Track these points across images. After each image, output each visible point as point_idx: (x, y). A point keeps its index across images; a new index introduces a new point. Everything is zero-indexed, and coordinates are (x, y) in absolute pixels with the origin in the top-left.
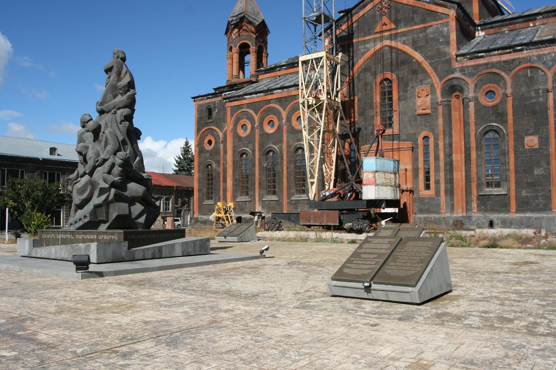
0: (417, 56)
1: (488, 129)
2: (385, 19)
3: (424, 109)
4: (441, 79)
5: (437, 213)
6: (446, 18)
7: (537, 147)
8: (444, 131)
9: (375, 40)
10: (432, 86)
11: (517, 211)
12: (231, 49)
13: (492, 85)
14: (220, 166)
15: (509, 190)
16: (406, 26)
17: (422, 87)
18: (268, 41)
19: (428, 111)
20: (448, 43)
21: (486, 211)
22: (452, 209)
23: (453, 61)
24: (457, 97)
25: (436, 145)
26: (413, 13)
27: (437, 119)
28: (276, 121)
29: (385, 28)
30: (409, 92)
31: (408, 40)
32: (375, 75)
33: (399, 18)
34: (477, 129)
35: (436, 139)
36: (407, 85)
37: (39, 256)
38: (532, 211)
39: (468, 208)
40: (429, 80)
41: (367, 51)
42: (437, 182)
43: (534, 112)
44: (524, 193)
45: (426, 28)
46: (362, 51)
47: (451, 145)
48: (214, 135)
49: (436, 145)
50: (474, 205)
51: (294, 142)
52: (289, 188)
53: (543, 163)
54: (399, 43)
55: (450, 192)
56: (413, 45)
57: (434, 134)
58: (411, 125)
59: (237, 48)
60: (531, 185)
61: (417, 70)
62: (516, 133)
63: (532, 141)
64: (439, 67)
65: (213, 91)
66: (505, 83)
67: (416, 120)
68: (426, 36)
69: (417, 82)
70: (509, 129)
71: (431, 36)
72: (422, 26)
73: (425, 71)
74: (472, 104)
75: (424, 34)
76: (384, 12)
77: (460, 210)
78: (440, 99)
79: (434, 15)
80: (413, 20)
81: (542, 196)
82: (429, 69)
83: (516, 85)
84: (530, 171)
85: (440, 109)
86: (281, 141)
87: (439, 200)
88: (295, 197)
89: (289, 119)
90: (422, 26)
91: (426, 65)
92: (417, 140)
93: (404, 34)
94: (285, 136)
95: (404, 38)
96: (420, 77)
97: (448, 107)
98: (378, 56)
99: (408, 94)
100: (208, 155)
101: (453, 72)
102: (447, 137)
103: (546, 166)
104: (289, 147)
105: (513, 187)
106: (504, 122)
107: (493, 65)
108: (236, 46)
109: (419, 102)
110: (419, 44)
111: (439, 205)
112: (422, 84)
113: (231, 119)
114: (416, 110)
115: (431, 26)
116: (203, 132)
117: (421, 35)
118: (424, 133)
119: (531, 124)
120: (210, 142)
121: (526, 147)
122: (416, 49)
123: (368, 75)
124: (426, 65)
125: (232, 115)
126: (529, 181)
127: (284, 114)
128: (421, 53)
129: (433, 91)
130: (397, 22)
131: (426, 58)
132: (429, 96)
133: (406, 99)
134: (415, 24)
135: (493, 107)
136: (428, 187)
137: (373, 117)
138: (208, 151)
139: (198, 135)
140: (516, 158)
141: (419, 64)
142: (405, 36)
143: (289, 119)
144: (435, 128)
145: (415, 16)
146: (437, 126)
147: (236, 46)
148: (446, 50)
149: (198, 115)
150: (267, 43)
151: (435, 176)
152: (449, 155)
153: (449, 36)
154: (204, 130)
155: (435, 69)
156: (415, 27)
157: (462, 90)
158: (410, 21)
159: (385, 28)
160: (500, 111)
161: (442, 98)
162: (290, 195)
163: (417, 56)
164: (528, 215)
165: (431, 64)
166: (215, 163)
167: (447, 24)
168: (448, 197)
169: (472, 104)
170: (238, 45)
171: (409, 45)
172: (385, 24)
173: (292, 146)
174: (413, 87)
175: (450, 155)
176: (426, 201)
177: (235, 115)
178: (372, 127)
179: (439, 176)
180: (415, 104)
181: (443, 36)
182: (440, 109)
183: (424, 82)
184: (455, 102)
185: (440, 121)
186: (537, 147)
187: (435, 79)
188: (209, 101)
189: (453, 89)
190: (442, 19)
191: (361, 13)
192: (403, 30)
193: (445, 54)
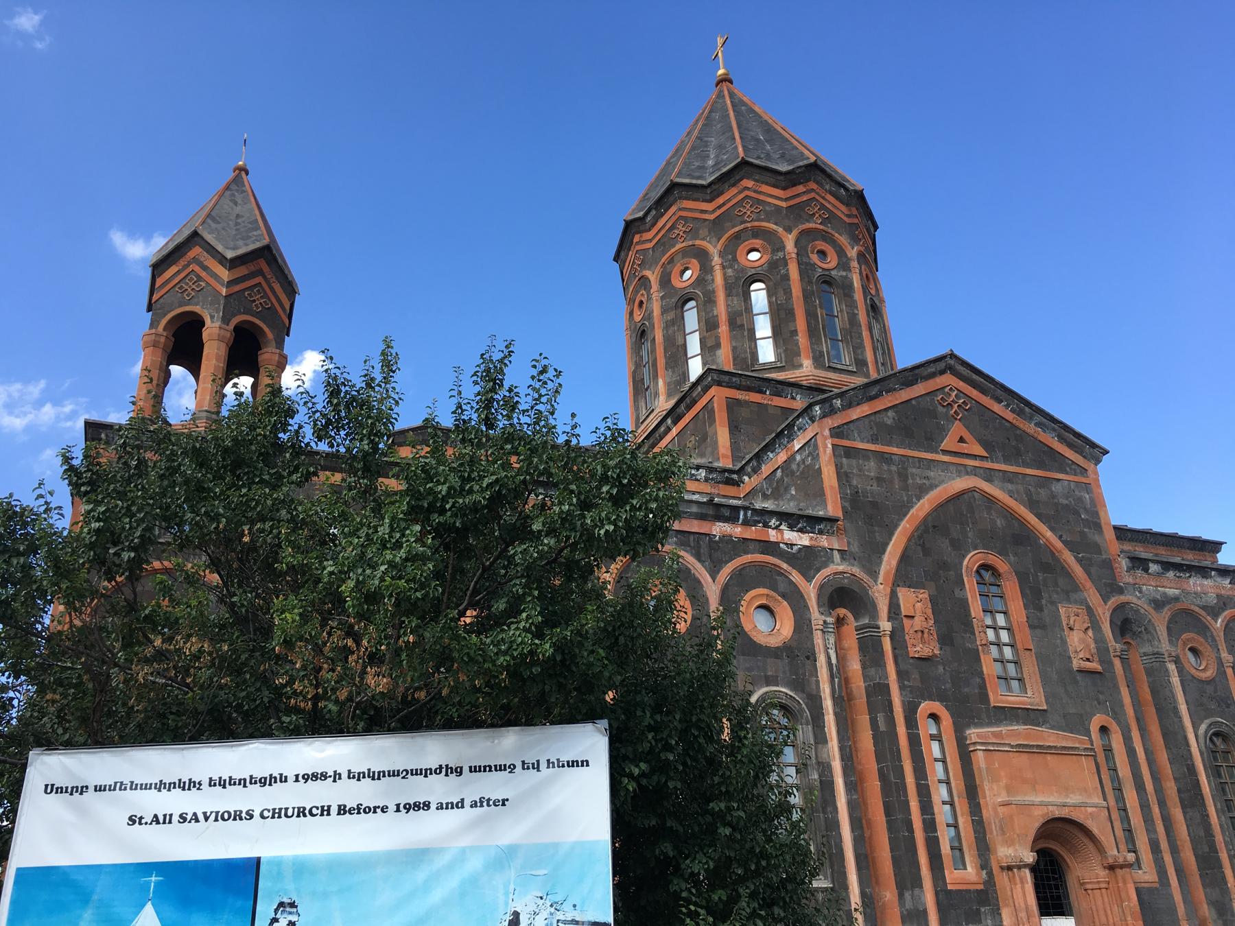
2: (957, 429)
3: (1088, 660)
4: (1105, 599)
6: (1082, 474)
10: (1090, 611)
16: (1007, 460)
27: (1116, 687)
29: (964, 448)
30: (1046, 611)
32: (960, 548)
35: (1127, 739)
49: (1131, 752)
57: (1119, 723)
59: (231, 327)
61: (1051, 565)
69: (1057, 593)
73: (1067, 574)
82: (1078, 570)
93: (1008, 478)
95: (1010, 486)
101: (1121, 591)
131: (1069, 545)
132: (1090, 633)
142: (1010, 481)
148: (1097, 538)
165: (1079, 561)
171: (1022, 502)
172: (962, 440)
174: (1053, 603)
179: (1156, 832)
180: (1064, 642)
187: (1092, 596)
192: (1004, 467)
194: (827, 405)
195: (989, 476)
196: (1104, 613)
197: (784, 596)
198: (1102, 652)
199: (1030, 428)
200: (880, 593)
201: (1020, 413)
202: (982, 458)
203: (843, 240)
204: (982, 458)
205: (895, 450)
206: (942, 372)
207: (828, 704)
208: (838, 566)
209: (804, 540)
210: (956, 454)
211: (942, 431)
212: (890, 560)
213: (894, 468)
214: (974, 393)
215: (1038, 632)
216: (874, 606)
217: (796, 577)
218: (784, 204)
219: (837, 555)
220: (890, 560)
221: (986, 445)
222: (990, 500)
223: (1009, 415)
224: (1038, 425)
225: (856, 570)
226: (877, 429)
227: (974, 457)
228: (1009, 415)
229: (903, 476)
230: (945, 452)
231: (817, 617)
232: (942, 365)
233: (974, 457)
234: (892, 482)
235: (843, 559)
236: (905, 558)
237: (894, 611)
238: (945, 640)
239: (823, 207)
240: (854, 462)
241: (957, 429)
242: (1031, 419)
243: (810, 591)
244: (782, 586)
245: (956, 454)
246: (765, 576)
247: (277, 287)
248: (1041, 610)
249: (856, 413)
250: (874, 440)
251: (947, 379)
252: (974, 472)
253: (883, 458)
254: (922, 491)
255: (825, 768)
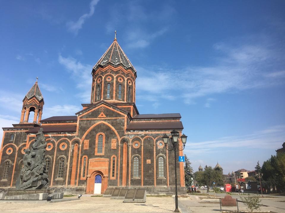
0: (113, 128)
1: (135, 156)
2: (102, 113)
4: (121, 137)
5: (116, 185)
7: (150, 163)
8: (120, 156)
9: (98, 120)
10: (117, 139)
11: (144, 185)
12: (25, 108)
13: (137, 141)
14: (14, 163)
15: (141, 178)
16: (110, 117)
17: (114, 139)
18: (43, 107)
19: (116, 148)
20: (124, 126)
21: (133, 185)
22: (121, 184)
23: (125, 132)
24: (126, 144)
25: (117, 161)
26: (113, 113)
27: (118, 151)
28: (52, 145)
29: (102, 116)
31: (110, 122)
32: (97, 132)
33: (108, 114)
34: (131, 156)
36: (108, 138)
37: (9, 199)
38: (148, 185)
39: (127, 184)
40: (117, 137)
41: (94, 124)
42: (117, 174)
43: (150, 152)
44: (146, 179)
45: (117, 119)
46: (93, 123)
47: (122, 161)
48: (13, 148)
49: (117, 161)
50: (129, 183)
51: (60, 155)
52: (54, 175)
53: (152, 169)
54: (107, 123)
55: (121, 178)
56: (112, 124)
58: (109, 152)
59: (29, 108)
60: (148, 176)
61: (112, 133)
62: (144, 158)
63: (149, 161)
64: (120, 133)
65: (13, 127)
66: (141, 141)
67: (111, 151)
68: (117, 121)
70: (142, 157)
71: (119, 122)
72: (115, 118)
73: (115, 134)
74: (130, 147)
75: (116, 121)
76: (102, 111)
77: (124, 185)
78: (120, 144)
79: (120, 115)
80: (112, 115)
81: (151, 180)
83: (144, 143)
84: (148, 171)
85: (120, 148)
86: (54, 155)
87: (117, 181)
88: (58, 179)
89: (58, 145)
90: (115, 118)
91: (116, 132)
92: (111, 158)
93: (109, 120)
94: (55, 152)
95: (109, 121)
96: (113, 135)
97: (122, 148)
98: (99, 126)
99: (109, 141)
100: (8, 157)
101: (125, 136)
102: (122, 158)
103: (153, 170)
104: (57, 157)
105: (142, 177)
106: (140, 154)
107: (138, 135)
108: (28, 108)
109: (112, 144)
110: (114, 124)
111: (117, 183)
112: (114, 138)
113: (29, 142)
114: (111, 147)
115: (118, 119)
116: (7, 146)
117: (115, 121)
118: (113, 156)
119: (149, 155)
120: (10, 151)
121: (147, 163)
122: (113, 126)
123: (94, 132)
124: (116, 132)
125: (30, 141)
126: (148, 175)
127: (56, 144)
128: (114, 127)
129: (117, 141)
130: (107, 115)
133: (107, 143)
134: (113, 117)
135: (137, 149)
136: (113, 176)
137: (94, 148)
138: (8, 155)
139: (3, 147)
140: (144, 167)
141: (113, 131)
142: (109, 120)
143: (58, 145)
144: (117, 154)
145: (113, 114)
146: (118, 153)
147: (28, 108)
148: (123, 127)
149: (5, 137)
150: (42, 109)
151: (116, 172)
152: (121, 164)
153: (124, 123)
154: (7, 145)
155: (119, 134)
156: (113, 118)
157: (127, 142)
158: (111, 116)
159: (102, 116)
160: (139, 150)
161: (121, 144)
162: (55, 177)
163: (113, 128)
164: (147, 186)
165: (118, 132)
166: (12, 161)
167: (124, 119)
168: (121, 180)
169: (130, 147)
170: (30, 108)
172: (102, 115)
173: (58, 157)
174: (111, 139)
175: (122, 164)
176: (113, 181)
177: (31, 141)
178: (94, 152)
180: (111, 145)
181: (122, 123)
182: (120, 148)
183: (115, 137)
184: (125, 145)
185: (120, 152)
186: (150, 163)
187: (118, 137)
188: (13, 131)
189: (124, 141)
190: (122, 117)
191: (93, 110)
192: (109, 118)
193: (123, 129)
194: (79, 114)
195: (105, 120)
196: (120, 140)
197: (66, 143)
198: (118, 146)
199: (116, 111)
200: (81, 141)
201: (114, 108)
202: (105, 117)
203: (113, 75)
204: (105, 117)
205: (90, 119)
206: (101, 104)
207: (69, 157)
208: (76, 138)
209: (70, 135)
210: (100, 118)
211: (99, 114)
212: (84, 136)
213: (89, 122)
214: (107, 107)
215: (106, 144)
216: (80, 143)
217: (69, 140)
218: (103, 71)
219: (76, 136)
220: (84, 136)
221: (106, 115)
222: (104, 124)
223: (112, 109)
224: (117, 110)
225: (79, 138)
226: (88, 116)
227: (104, 117)
228: (112, 109)
229: (90, 123)
230: (98, 118)
231: (70, 146)
232: (101, 103)
233: (104, 117)
234: (88, 124)
235: (77, 137)
236: (87, 135)
237: (83, 143)
238: (90, 146)
239: (111, 70)
240: (82, 122)
241: (102, 113)
242: (115, 109)
243: (70, 142)
244: (67, 141)
245: (100, 118)
246: (64, 141)
247: (36, 100)
248: (108, 140)
249: (84, 114)
250: (87, 118)
251: (103, 105)
252: (103, 120)
253: (88, 120)
254: (93, 124)
255: (67, 165)
